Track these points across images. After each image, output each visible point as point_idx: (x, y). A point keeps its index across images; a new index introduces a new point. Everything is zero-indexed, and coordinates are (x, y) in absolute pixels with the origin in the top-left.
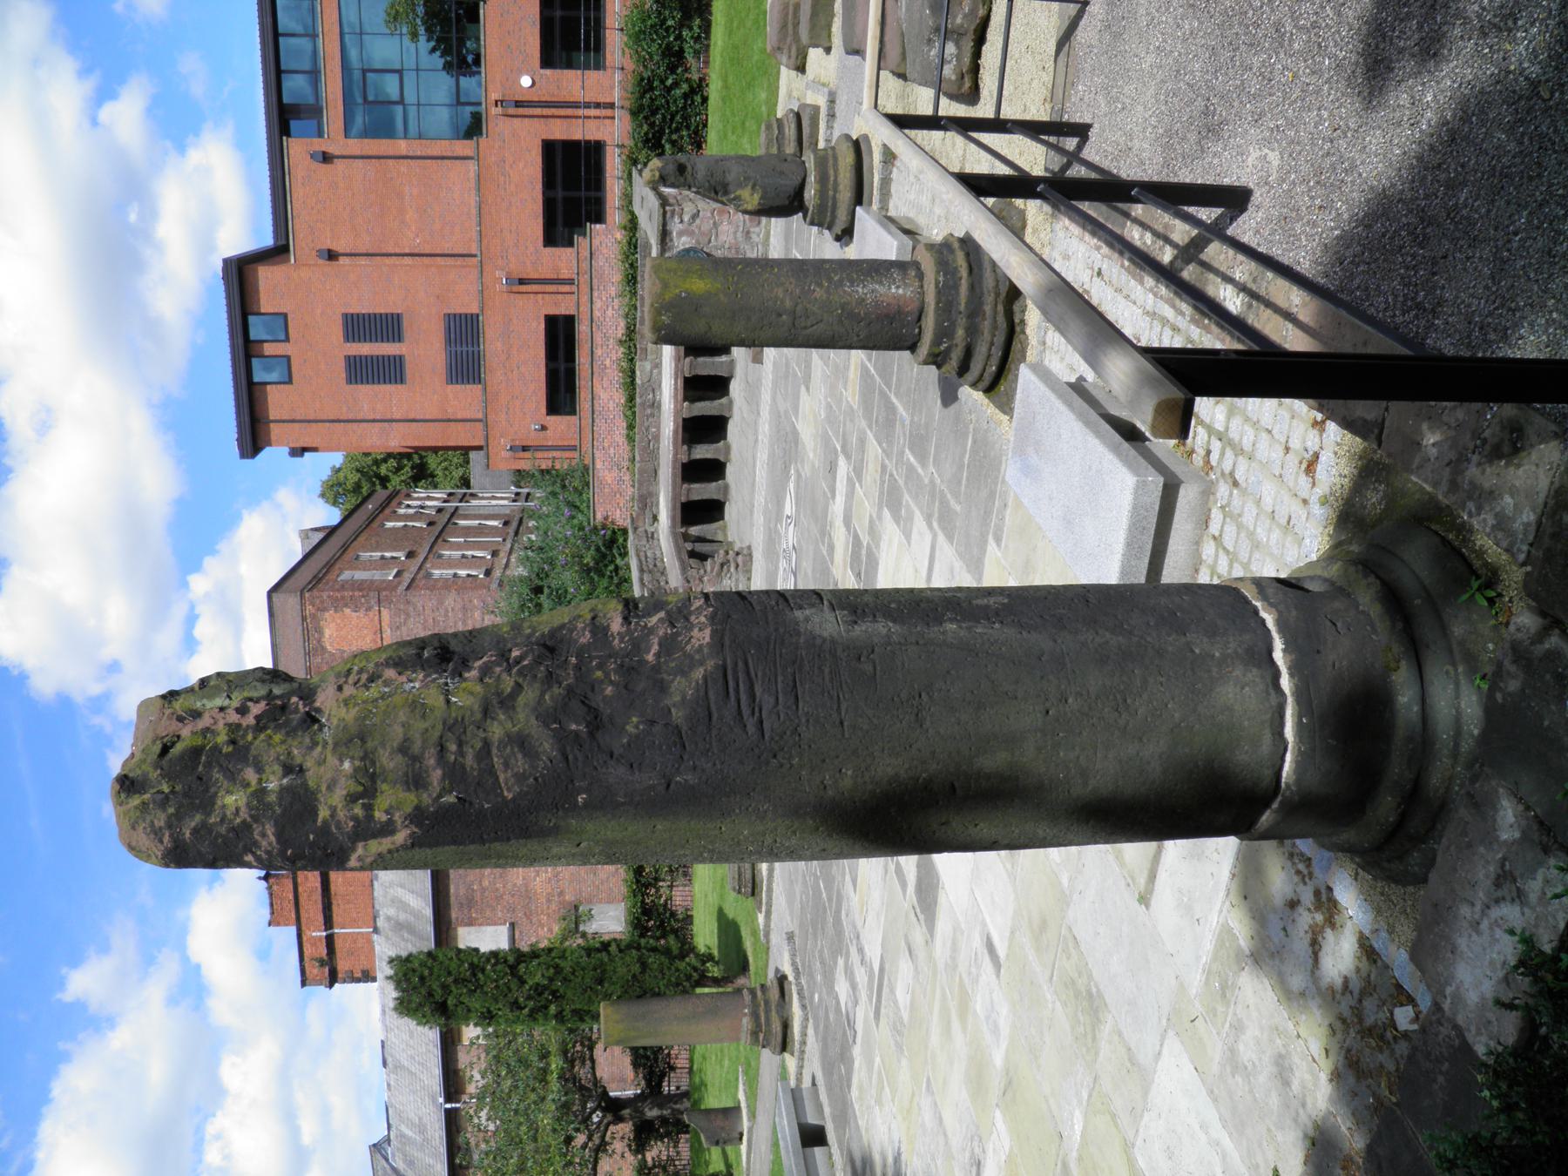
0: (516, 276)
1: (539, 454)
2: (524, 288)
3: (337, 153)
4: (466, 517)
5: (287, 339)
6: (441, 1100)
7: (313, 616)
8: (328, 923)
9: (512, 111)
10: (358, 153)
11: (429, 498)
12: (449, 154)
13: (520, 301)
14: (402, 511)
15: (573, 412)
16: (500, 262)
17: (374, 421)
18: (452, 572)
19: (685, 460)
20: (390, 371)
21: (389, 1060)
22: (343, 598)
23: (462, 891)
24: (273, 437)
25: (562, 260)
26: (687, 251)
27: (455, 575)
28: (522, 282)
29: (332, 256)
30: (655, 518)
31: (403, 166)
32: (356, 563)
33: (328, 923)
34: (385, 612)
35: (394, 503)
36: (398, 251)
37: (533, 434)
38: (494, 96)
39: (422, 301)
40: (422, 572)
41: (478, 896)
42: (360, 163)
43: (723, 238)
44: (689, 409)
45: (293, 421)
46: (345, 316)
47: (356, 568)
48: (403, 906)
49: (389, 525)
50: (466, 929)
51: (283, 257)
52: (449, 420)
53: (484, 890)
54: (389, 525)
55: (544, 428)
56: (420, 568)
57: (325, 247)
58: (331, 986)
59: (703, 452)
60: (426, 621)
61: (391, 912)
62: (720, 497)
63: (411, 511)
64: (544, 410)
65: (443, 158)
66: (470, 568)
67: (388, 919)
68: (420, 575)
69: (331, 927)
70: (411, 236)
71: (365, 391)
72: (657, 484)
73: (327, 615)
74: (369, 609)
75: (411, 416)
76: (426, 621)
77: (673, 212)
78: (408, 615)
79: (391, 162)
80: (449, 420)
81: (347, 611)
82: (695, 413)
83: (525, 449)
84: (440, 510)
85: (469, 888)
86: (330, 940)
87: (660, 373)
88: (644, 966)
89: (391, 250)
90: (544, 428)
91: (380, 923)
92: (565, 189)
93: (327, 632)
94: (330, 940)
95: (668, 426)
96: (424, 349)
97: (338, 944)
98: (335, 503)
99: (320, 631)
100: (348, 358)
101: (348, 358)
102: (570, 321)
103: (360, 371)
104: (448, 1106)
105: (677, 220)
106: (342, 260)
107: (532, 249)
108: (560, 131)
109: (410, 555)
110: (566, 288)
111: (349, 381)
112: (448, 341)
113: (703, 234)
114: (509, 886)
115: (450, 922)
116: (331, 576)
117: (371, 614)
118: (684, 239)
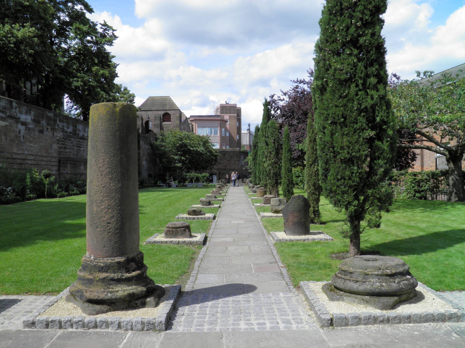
88: (349, 161)
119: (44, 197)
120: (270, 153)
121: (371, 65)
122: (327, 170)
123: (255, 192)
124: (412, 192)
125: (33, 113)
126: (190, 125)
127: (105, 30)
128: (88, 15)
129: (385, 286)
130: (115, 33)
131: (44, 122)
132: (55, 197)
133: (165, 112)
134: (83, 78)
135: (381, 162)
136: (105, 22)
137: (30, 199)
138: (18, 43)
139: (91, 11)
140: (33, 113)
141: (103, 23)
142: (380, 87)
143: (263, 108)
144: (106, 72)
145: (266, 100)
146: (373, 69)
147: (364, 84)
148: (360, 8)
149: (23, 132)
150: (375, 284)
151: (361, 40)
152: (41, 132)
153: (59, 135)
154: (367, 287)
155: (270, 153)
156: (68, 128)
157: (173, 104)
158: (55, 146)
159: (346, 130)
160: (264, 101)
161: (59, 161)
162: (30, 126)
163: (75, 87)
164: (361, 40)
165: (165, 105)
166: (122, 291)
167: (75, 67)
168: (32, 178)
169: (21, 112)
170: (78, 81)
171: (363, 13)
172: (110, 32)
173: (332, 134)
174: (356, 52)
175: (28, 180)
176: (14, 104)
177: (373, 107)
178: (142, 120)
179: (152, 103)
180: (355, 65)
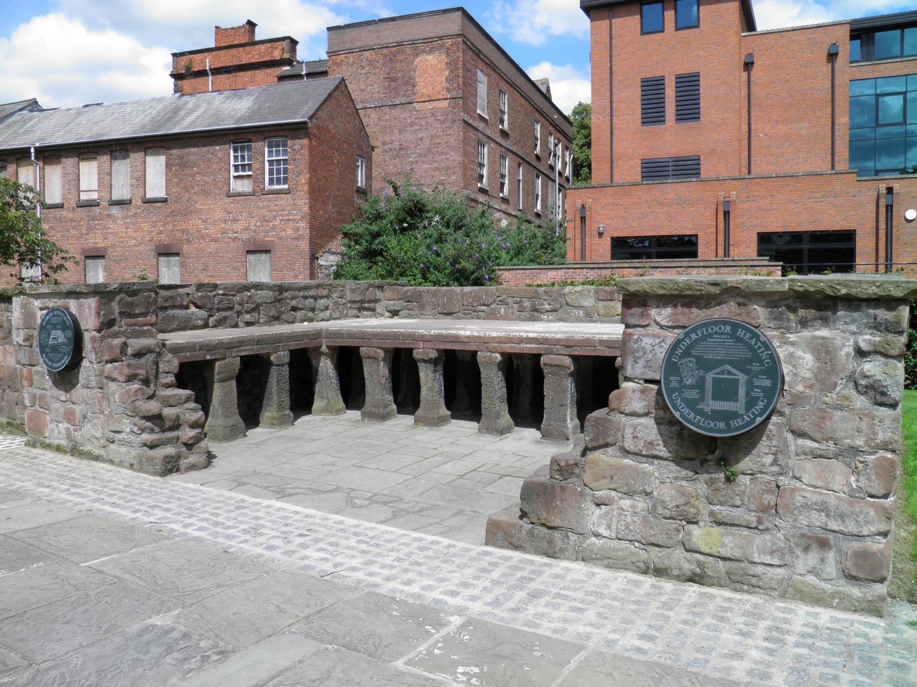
0: (732, 209)
1: (578, 232)
2: (721, 215)
3: (837, 65)
4: (545, 186)
5: (677, 29)
6: (37, 145)
7: (443, 46)
8: (216, 71)
9: (883, 202)
10: (837, 83)
11: (564, 164)
12: (836, 159)
13: (710, 213)
14: (552, 140)
15: (614, 256)
16: (744, 195)
17: (611, 102)
18: (486, 162)
19: (417, 354)
20: (652, 113)
21: (87, 109)
22: (458, 69)
24: (598, 23)
25: (746, 247)
26: (773, 369)
27: (481, 165)
28: (727, 214)
29: (748, 66)
30: (395, 313)
31: (826, 121)
32: (495, 92)
33: (216, 71)
34: (445, 103)
35: (559, 135)
36: (753, 119)
37: (595, 226)
38: (896, 186)
39: (711, 137)
40: (485, 139)
41: (188, 171)
42: (828, 85)
43: (809, 471)
44: (490, 362)
45: (611, 37)
46: (697, 75)
47: (490, 86)
48: (189, 114)
49: (538, 127)
50: (164, 163)
51: (745, 28)
52: (612, 162)
53: (193, 176)
54: (538, 127)
55: (601, 235)
56: (488, 137)
57: (755, 60)
58: (172, 75)
59: (430, 382)
60: (438, 137)
61: (190, 105)
62: (367, 407)
63: (552, 147)
64: (616, 235)
65: (833, 154)
66: (489, 178)
67: (186, 104)
68: (481, 136)
69: (213, 74)
70: (766, 130)
71: (636, 93)
72: (434, 316)
73: (444, 56)
74: (448, 90)
75: (615, 132)
76: (438, 137)
77: (892, 328)
78: (443, 122)
79: (829, 110)
80: (612, 162)
81: (447, 73)
82: (484, 373)
83: (583, 219)
84: (552, 168)
85: (195, 164)
86: (203, 73)
87: (578, 320)
89: (753, 114)
90: (601, 235)
91: (186, 98)
92: (810, 250)
93: (430, 57)
94: (203, 73)
95: (467, 329)
96: (671, 139)
97: (201, 80)
98: (575, 113)
99: (431, 52)
100: (662, 79)
101: (662, 79)
102: (694, 254)
103: (652, 90)
104: (32, 150)
105: (866, 339)
106: (744, 75)
107: (756, 222)
108: (864, 246)
109: (504, 134)
110: (721, 252)
111: (643, 81)
112: (677, 160)
113: (823, 416)
114: (195, 198)
115: (169, 148)
116: (481, 65)
117: (445, 92)
118: (808, 359)
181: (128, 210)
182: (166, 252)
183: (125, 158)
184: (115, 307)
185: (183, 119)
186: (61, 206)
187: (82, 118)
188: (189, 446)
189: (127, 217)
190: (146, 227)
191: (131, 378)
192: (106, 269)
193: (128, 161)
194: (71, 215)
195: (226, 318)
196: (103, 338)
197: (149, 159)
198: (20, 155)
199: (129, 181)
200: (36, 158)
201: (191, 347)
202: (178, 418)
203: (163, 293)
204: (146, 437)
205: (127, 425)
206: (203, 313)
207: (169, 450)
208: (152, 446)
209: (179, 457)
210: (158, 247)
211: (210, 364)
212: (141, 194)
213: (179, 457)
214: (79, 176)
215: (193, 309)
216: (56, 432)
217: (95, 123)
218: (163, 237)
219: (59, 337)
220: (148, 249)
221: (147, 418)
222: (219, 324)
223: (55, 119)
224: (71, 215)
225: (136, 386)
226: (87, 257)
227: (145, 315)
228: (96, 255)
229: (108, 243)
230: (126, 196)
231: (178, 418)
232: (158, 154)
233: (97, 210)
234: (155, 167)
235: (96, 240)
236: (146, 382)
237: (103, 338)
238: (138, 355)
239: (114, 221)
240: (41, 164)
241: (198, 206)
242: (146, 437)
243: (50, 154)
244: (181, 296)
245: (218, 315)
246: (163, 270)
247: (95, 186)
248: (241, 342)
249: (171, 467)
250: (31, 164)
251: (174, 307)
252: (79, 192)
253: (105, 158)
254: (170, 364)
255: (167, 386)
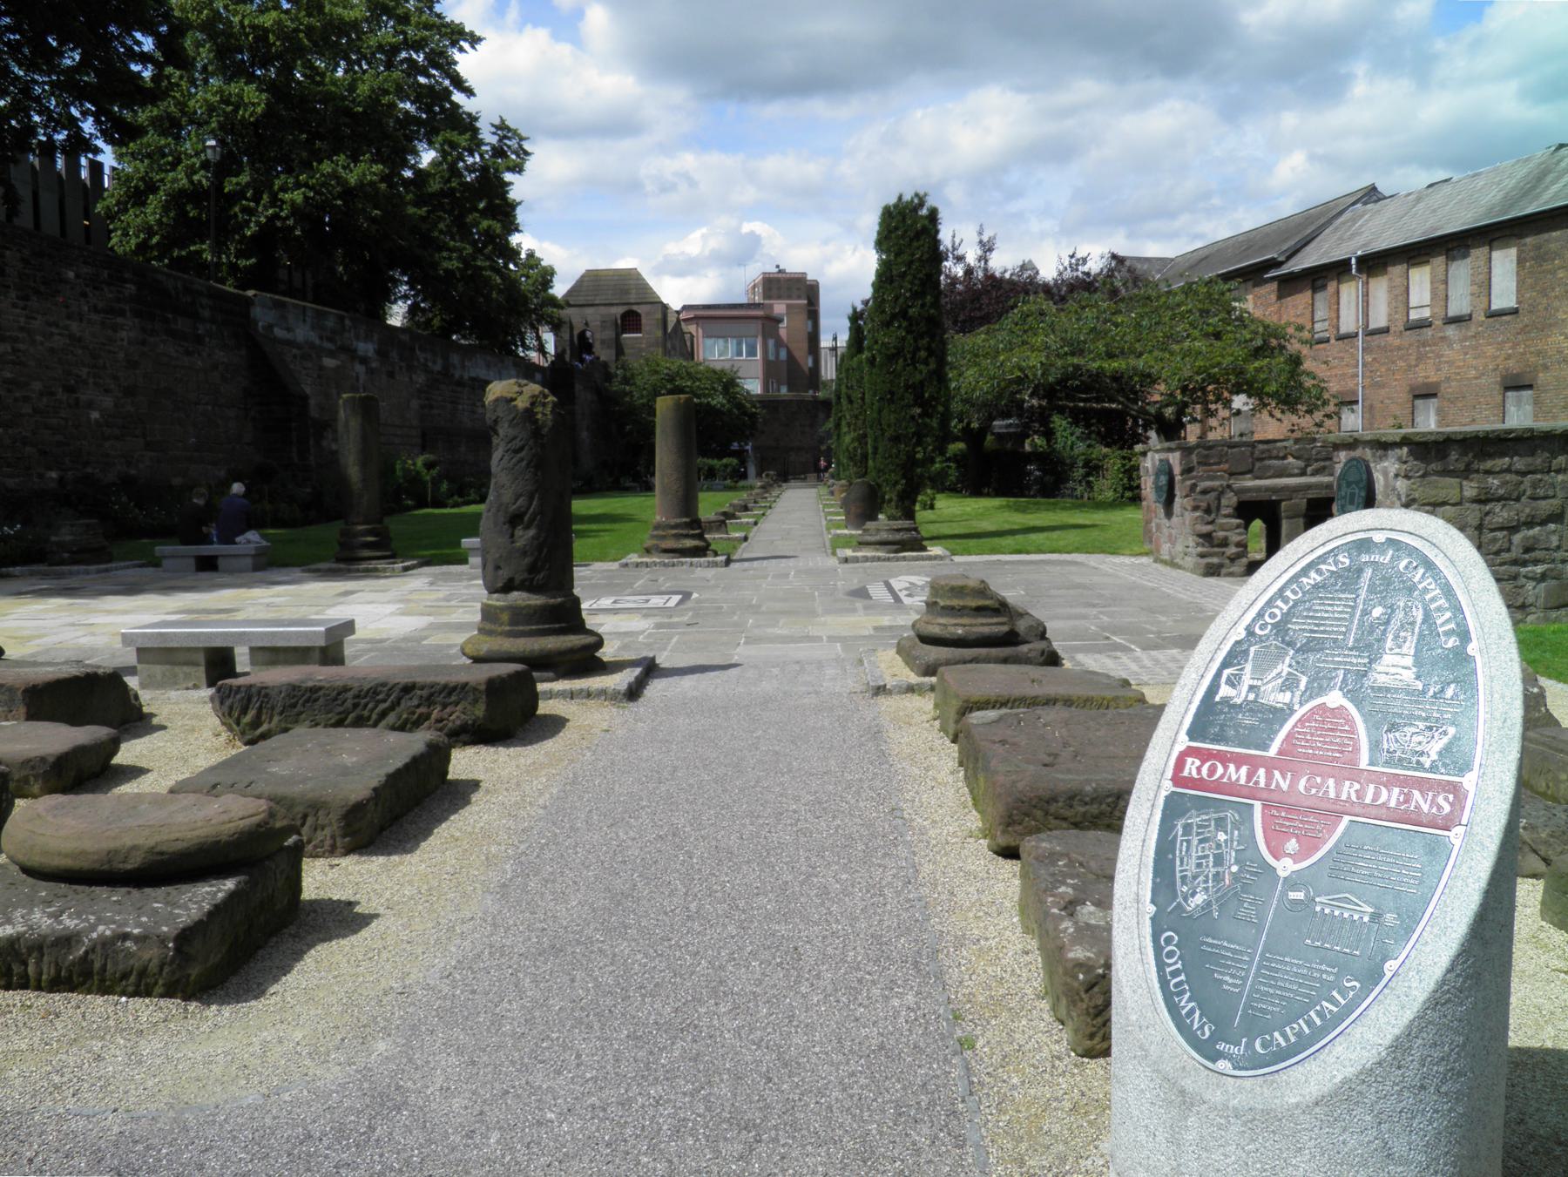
23: (1553, 246)
41: (1547, 266)
53: (1553, 272)
88: (896, 439)
114: (1556, 303)
115: (1521, 236)
119: (426, 506)
120: (856, 417)
121: (922, 337)
122: (876, 449)
123: (832, 493)
124: (1120, 489)
125: (376, 337)
126: (687, 337)
127: (500, 141)
128: (458, 97)
129: (891, 537)
130: (527, 146)
131: (394, 355)
132: (444, 506)
133: (625, 308)
134: (460, 250)
135: (929, 440)
136: (503, 121)
137: (409, 509)
138: (349, 193)
139: (469, 92)
140: (376, 337)
141: (497, 122)
142: (932, 360)
143: (848, 324)
144: (497, 227)
145: (855, 309)
146: (925, 341)
147: (913, 358)
148: (909, 278)
149: (362, 377)
150: (884, 536)
151: (911, 311)
152: (391, 375)
153: (420, 379)
154: (877, 538)
155: (856, 417)
156: (434, 363)
157: (644, 288)
158: (415, 404)
159: (893, 407)
160: (850, 311)
161: (424, 435)
162: (374, 365)
163: (446, 271)
164: (911, 311)
165: (627, 292)
166: (689, 543)
167: (442, 226)
168: (403, 469)
169: (357, 338)
170: (450, 259)
171: (912, 283)
172: (513, 143)
173: (880, 411)
174: (905, 324)
175: (399, 473)
176: (347, 322)
177: (921, 382)
178: (571, 328)
179: (594, 285)
180: (903, 339)
181: (1468, 328)
182: (1515, 384)
183: (1465, 256)
184: (1194, 458)
185: (1547, 188)
186: (1386, 330)
187: (1421, 205)
188: (1232, 560)
189: (1465, 339)
190: (1490, 350)
191: (1195, 508)
192: (1439, 412)
193: (1469, 260)
194: (1397, 342)
195: (1324, 468)
196: (1183, 481)
197: (1496, 255)
198: (1339, 269)
199: (1469, 289)
200: (1359, 270)
201: (1249, 490)
202: (1226, 538)
203: (1261, 447)
204: (1200, 549)
205: (1191, 541)
206: (1301, 463)
207: (1215, 560)
208: (1202, 556)
209: (1221, 566)
210: (1504, 378)
211: (1278, 502)
212: (1484, 305)
213: (1221, 566)
214: (1408, 288)
215: (1291, 460)
216: (1165, 548)
217: (1434, 211)
218: (1511, 363)
219: (1163, 480)
220: (1491, 381)
221: (1200, 536)
222: (1316, 473)
223: (1388, 210)
224: (1397, 342)
225: (1198, 514)
226: (1416, 397)
227: (1219, 464)
228: (1426, 393)
229: (1442, 375)
230: (1466, 310)
231: (1226, 538)
232: (1507, 246)
233: (1429, 332)
234: (1504, 263)
235: (1427, 373)
236: (1208, 511)
237: (1183, 481)
238: (1205, 492)
239: (1450, 346)
240: (1364, 277)
241: (1561, 316)
242: (1200, 549)
243: (1375, 263)
244: (1279, 449)
245: (1316, 465)
246: (1511, 409)
247: (1427, 301)
248: (1309, 487)
249: (1212, 571)
250: (1353, 278)
251: (1270, 458)
252: (1408, 309)
253: (1439, 261)
254: (1230, 500)
255: (1226, 516)
